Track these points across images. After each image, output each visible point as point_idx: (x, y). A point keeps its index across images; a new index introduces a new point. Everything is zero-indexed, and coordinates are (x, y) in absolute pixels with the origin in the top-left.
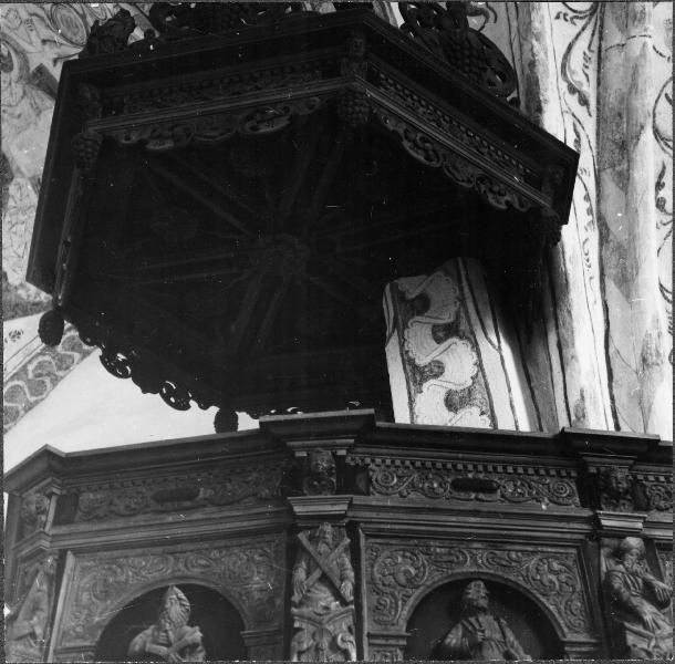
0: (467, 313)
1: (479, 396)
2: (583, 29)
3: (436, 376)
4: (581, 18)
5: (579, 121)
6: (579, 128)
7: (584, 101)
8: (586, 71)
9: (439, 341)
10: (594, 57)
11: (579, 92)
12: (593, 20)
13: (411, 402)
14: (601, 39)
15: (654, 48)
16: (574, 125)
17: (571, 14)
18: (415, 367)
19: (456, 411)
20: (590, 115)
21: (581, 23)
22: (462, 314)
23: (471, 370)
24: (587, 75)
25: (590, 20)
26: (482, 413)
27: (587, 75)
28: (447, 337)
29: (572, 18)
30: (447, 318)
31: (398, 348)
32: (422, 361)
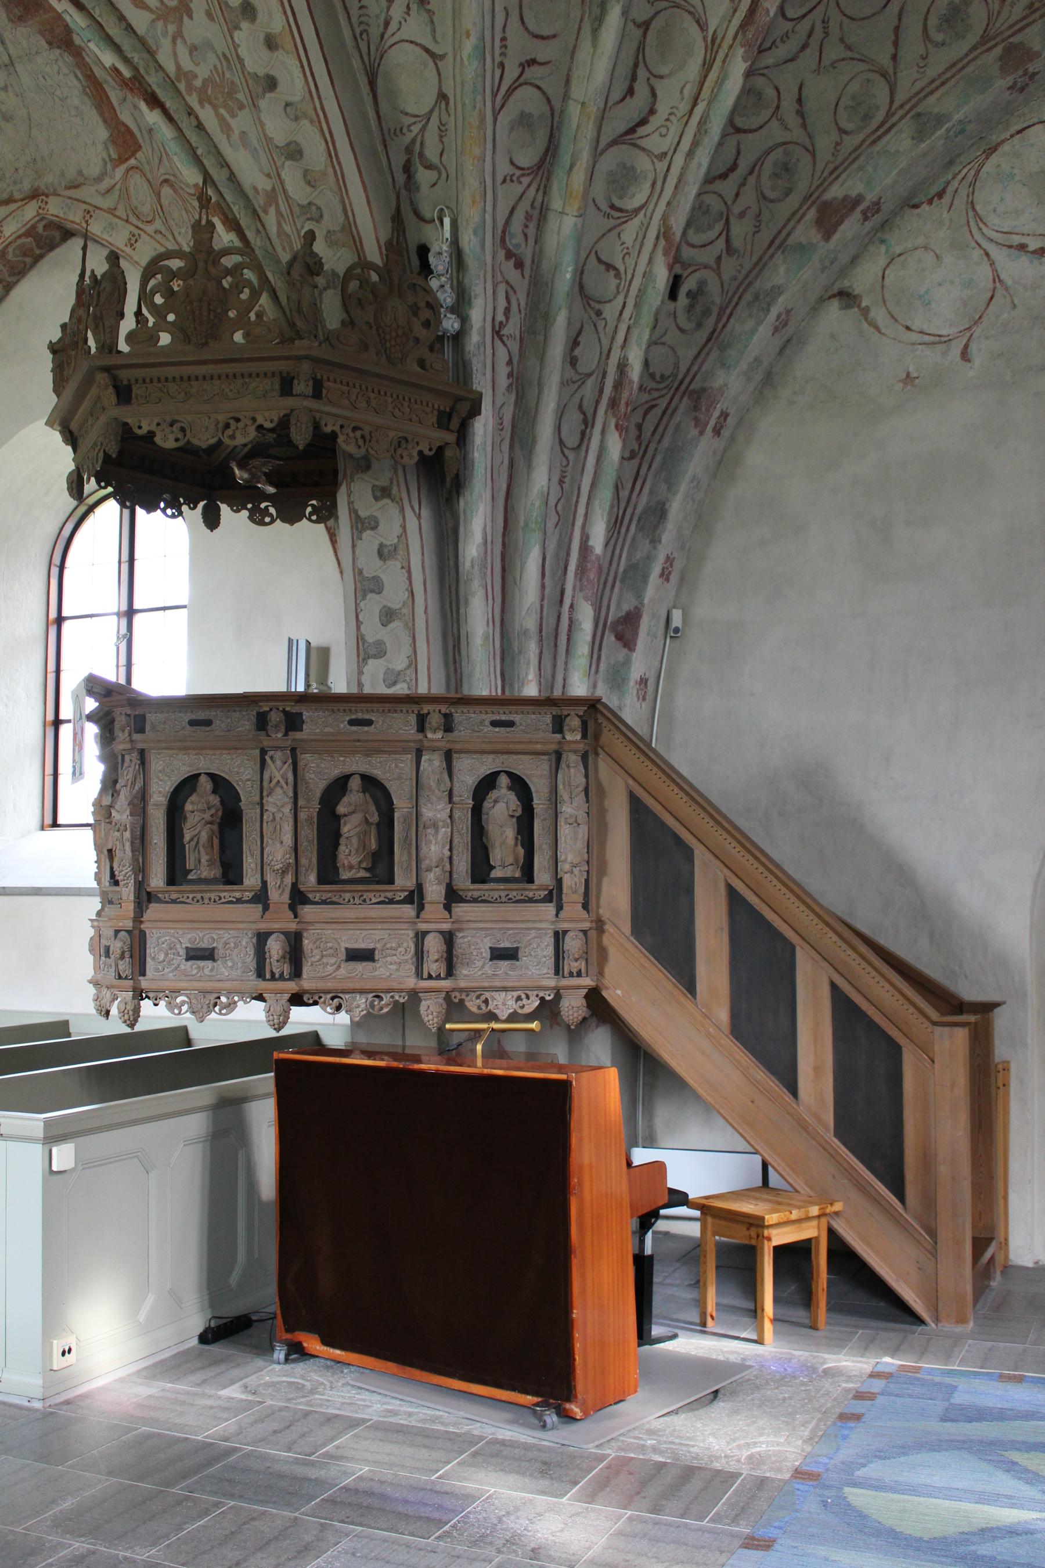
0: (398, 481)
1: (401, 553)
2: (529, 186)
3: (373, 529)
4: (528, 174)
5: (512, 287)
6: (511, 294)
7: (519, 265)
8: (526, 231)
9: (376, 499)
10: (536, 213)
11: (515, 255)
12: (539, 178)
13: (354, 546)
14: (545, 193)
15: (594, 201)
16: (507, 292)
17: (518, 173)
18: (358, 517)
19: (385, 560)
20: (523, 276)
21: (526, 181)
22: (395, 482)
23: (397, 530)
24: (526, 235)
25: (534, 178)
26: (403, 568)
27: (526, 235)
28: (383, 497)
29: (518, 178)
30: (383, 482)
31: (346, 498)
32: (363, 514)
